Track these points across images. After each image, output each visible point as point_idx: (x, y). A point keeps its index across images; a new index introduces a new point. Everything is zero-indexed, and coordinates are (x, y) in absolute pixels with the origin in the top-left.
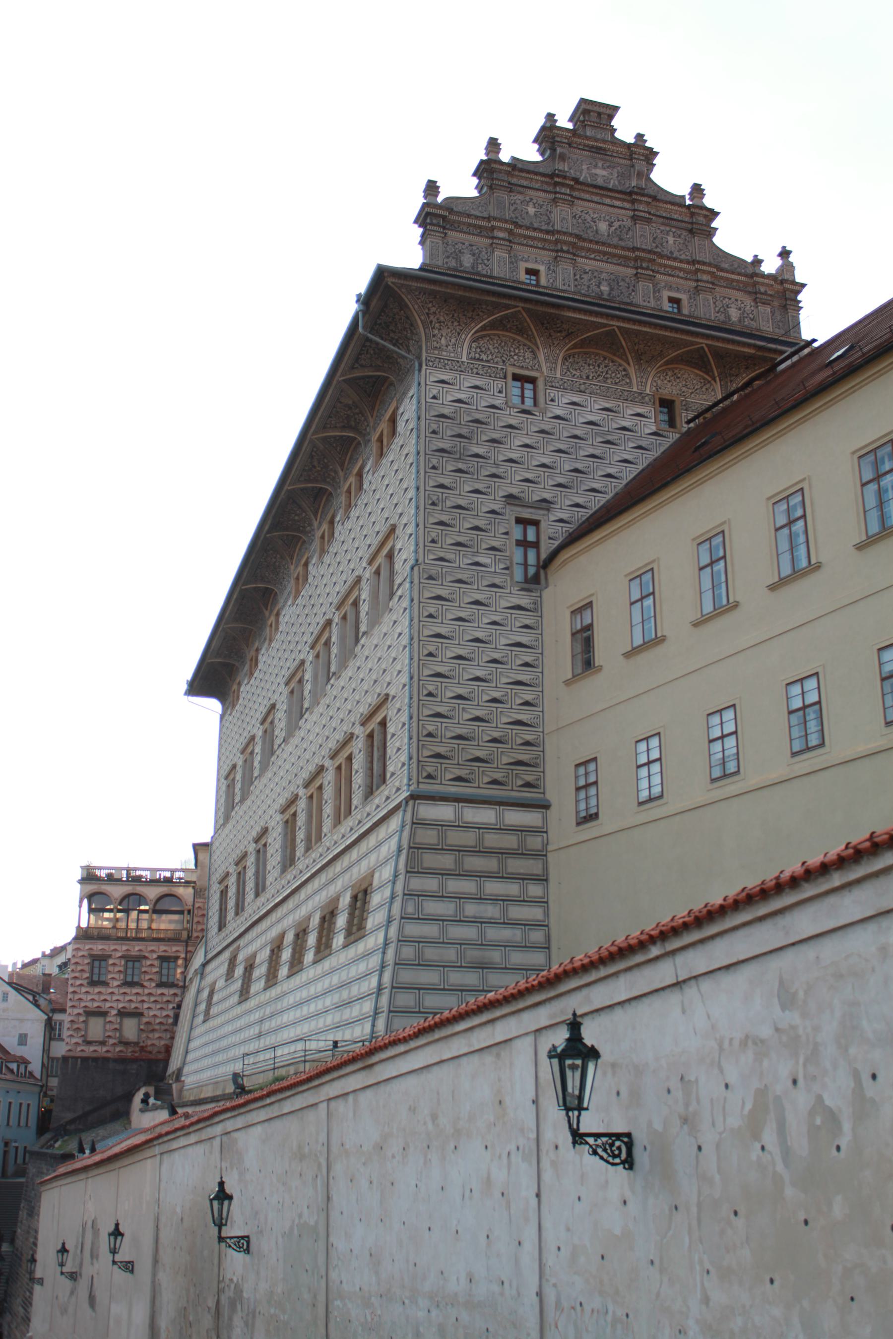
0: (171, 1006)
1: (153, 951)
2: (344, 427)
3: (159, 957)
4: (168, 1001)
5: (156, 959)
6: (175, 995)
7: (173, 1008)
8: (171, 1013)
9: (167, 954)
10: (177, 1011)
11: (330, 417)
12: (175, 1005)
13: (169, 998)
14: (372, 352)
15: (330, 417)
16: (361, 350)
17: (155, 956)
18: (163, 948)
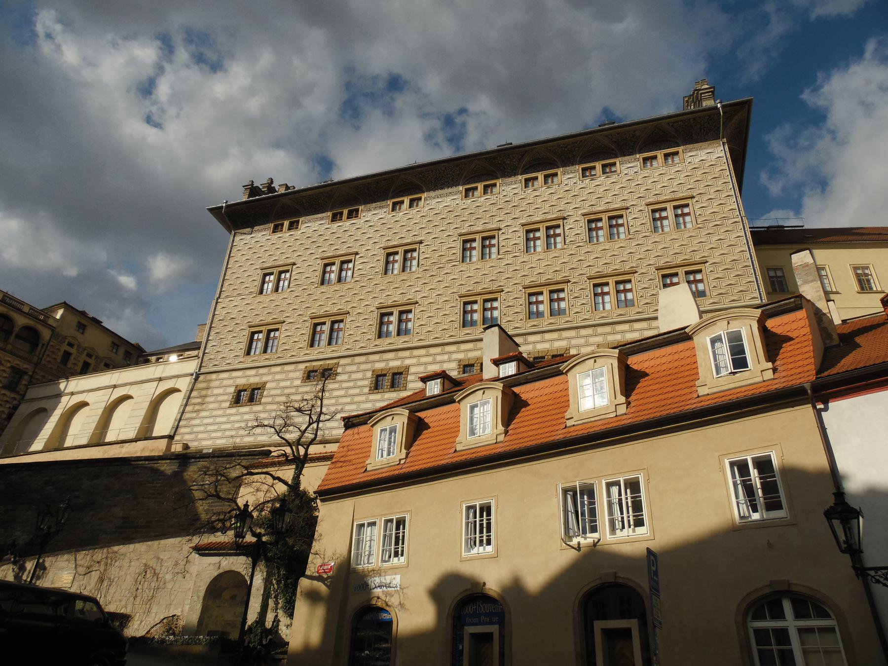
0: (8, 406)
1: (8, 361)
2: (615, 142)
3: (12, 367)
4: (7, 401)
5: (9, 367)
6: (14, 398)
7: (10, 407)
8: (7, 411)
9: (18, 367)
10: (13, 411)
11: (618, 134)
12: (11, 406)
13: (8, 399)
14: (686, 124)
15: (618, 134)
16: (685, 120)
17: (9, 365)
18: (17, 362)
